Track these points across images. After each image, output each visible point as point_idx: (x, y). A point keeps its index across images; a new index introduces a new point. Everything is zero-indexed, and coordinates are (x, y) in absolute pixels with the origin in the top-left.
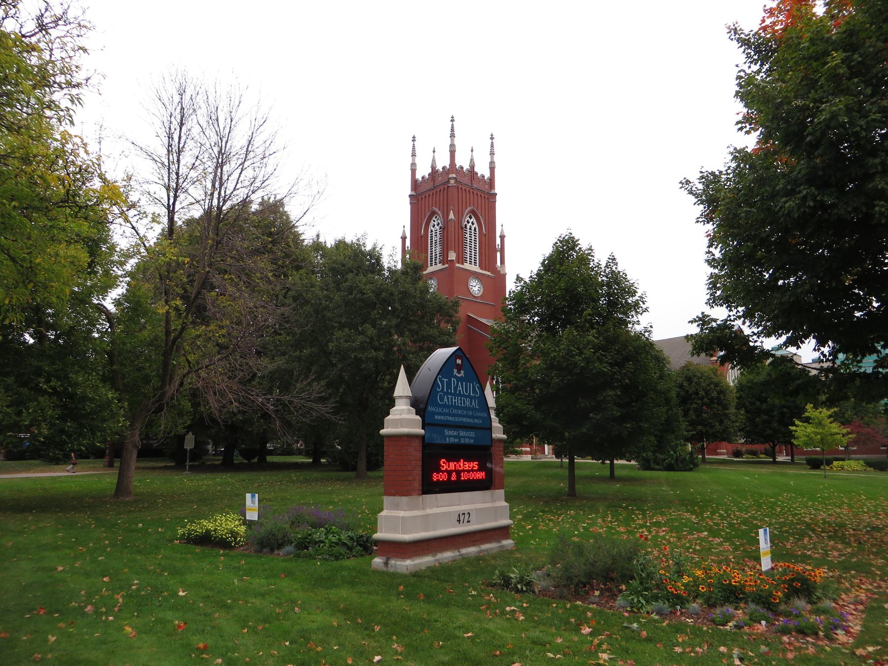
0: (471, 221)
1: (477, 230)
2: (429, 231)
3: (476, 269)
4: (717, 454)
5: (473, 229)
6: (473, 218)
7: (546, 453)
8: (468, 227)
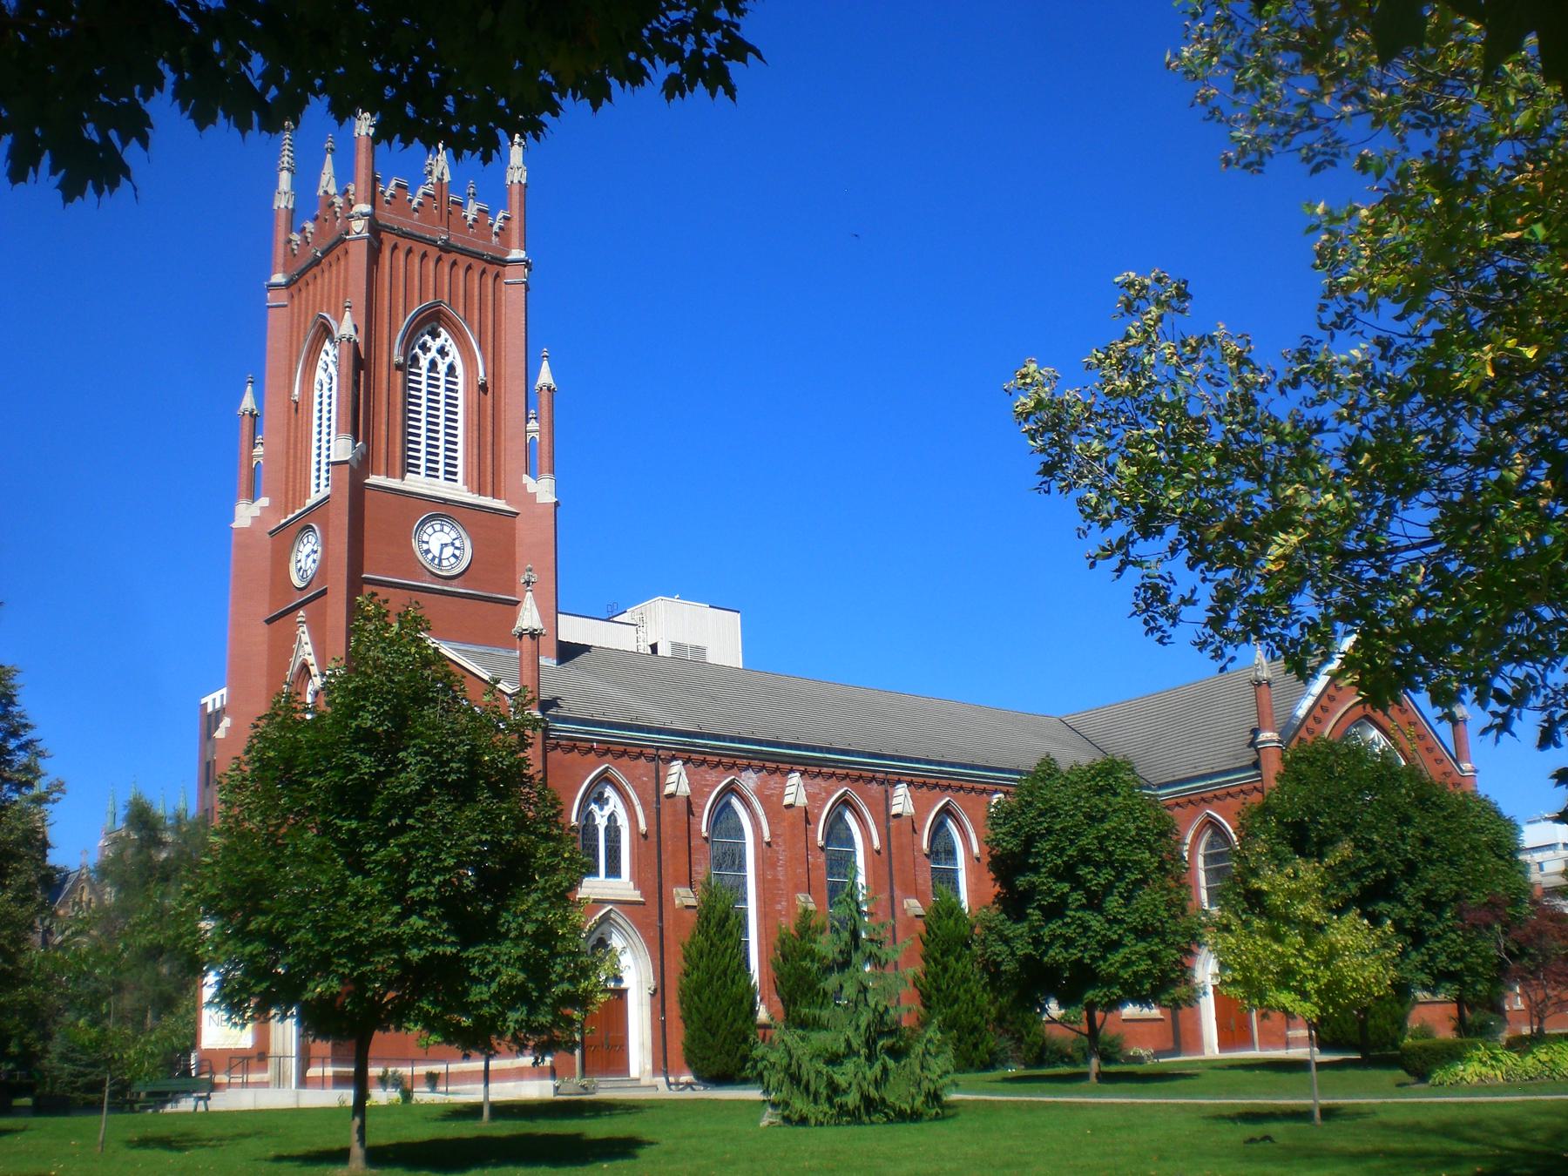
0: (434, 345)
1: (460, 370)
2: (317, 386)
3: (459, 491)
4: (1287, 1044)
5: (442, 368)
6: (444, 334)
7: (634, 1071)
8: (424, 362)
